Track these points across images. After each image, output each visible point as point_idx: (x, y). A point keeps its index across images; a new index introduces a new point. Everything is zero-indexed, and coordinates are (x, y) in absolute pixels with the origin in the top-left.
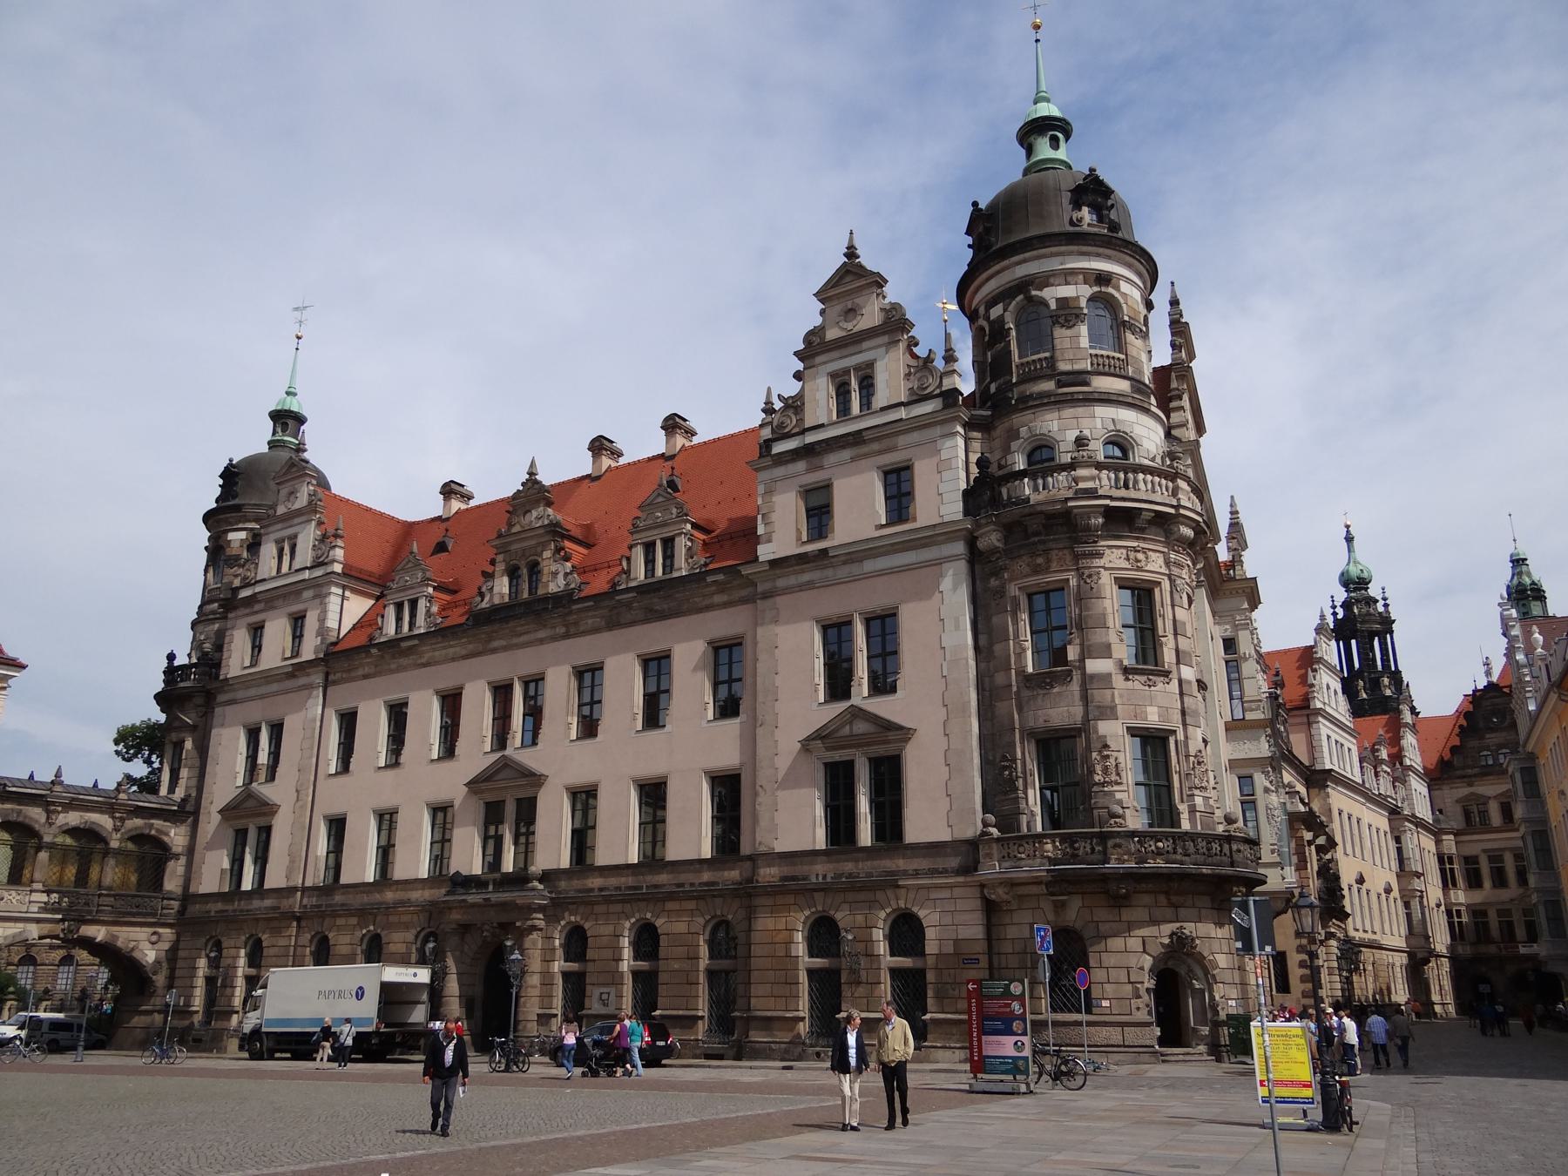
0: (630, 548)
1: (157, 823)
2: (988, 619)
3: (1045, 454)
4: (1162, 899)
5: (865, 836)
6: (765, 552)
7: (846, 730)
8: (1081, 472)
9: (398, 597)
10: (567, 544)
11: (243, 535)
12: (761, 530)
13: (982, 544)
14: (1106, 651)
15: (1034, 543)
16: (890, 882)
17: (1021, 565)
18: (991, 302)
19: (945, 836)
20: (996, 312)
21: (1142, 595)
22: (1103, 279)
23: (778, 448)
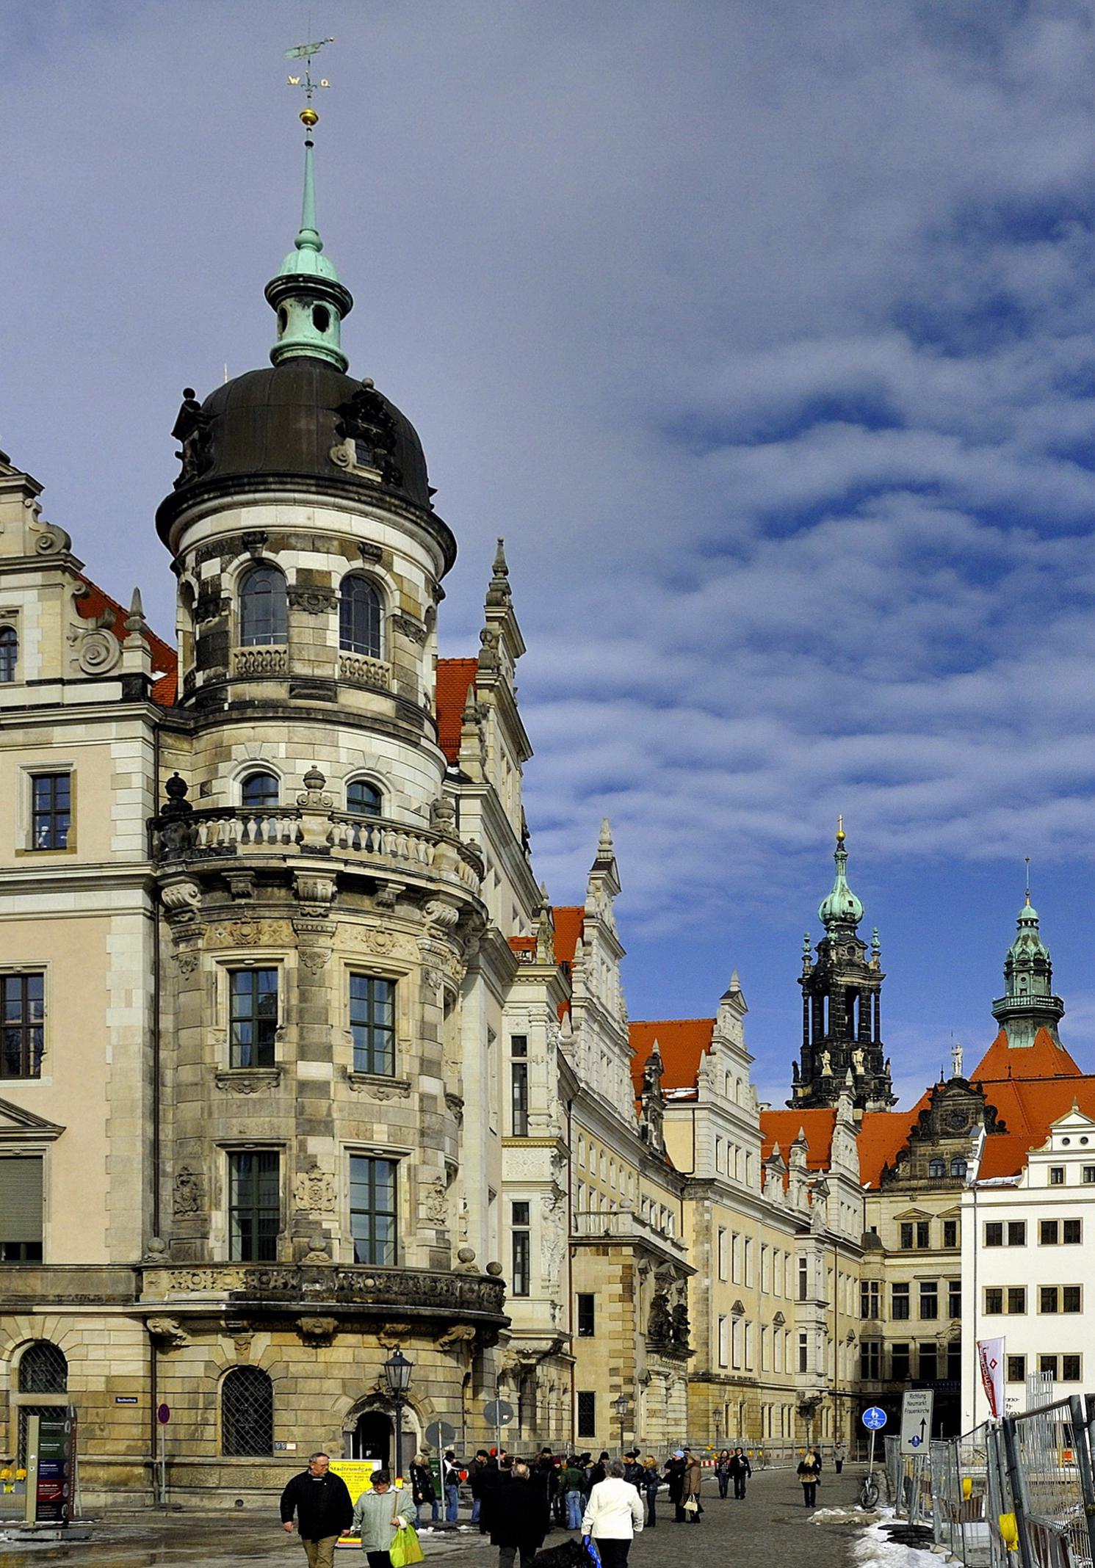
4: (372, 1339)
13: (168, 895)
15: (240, 906)
20: (211, 568)
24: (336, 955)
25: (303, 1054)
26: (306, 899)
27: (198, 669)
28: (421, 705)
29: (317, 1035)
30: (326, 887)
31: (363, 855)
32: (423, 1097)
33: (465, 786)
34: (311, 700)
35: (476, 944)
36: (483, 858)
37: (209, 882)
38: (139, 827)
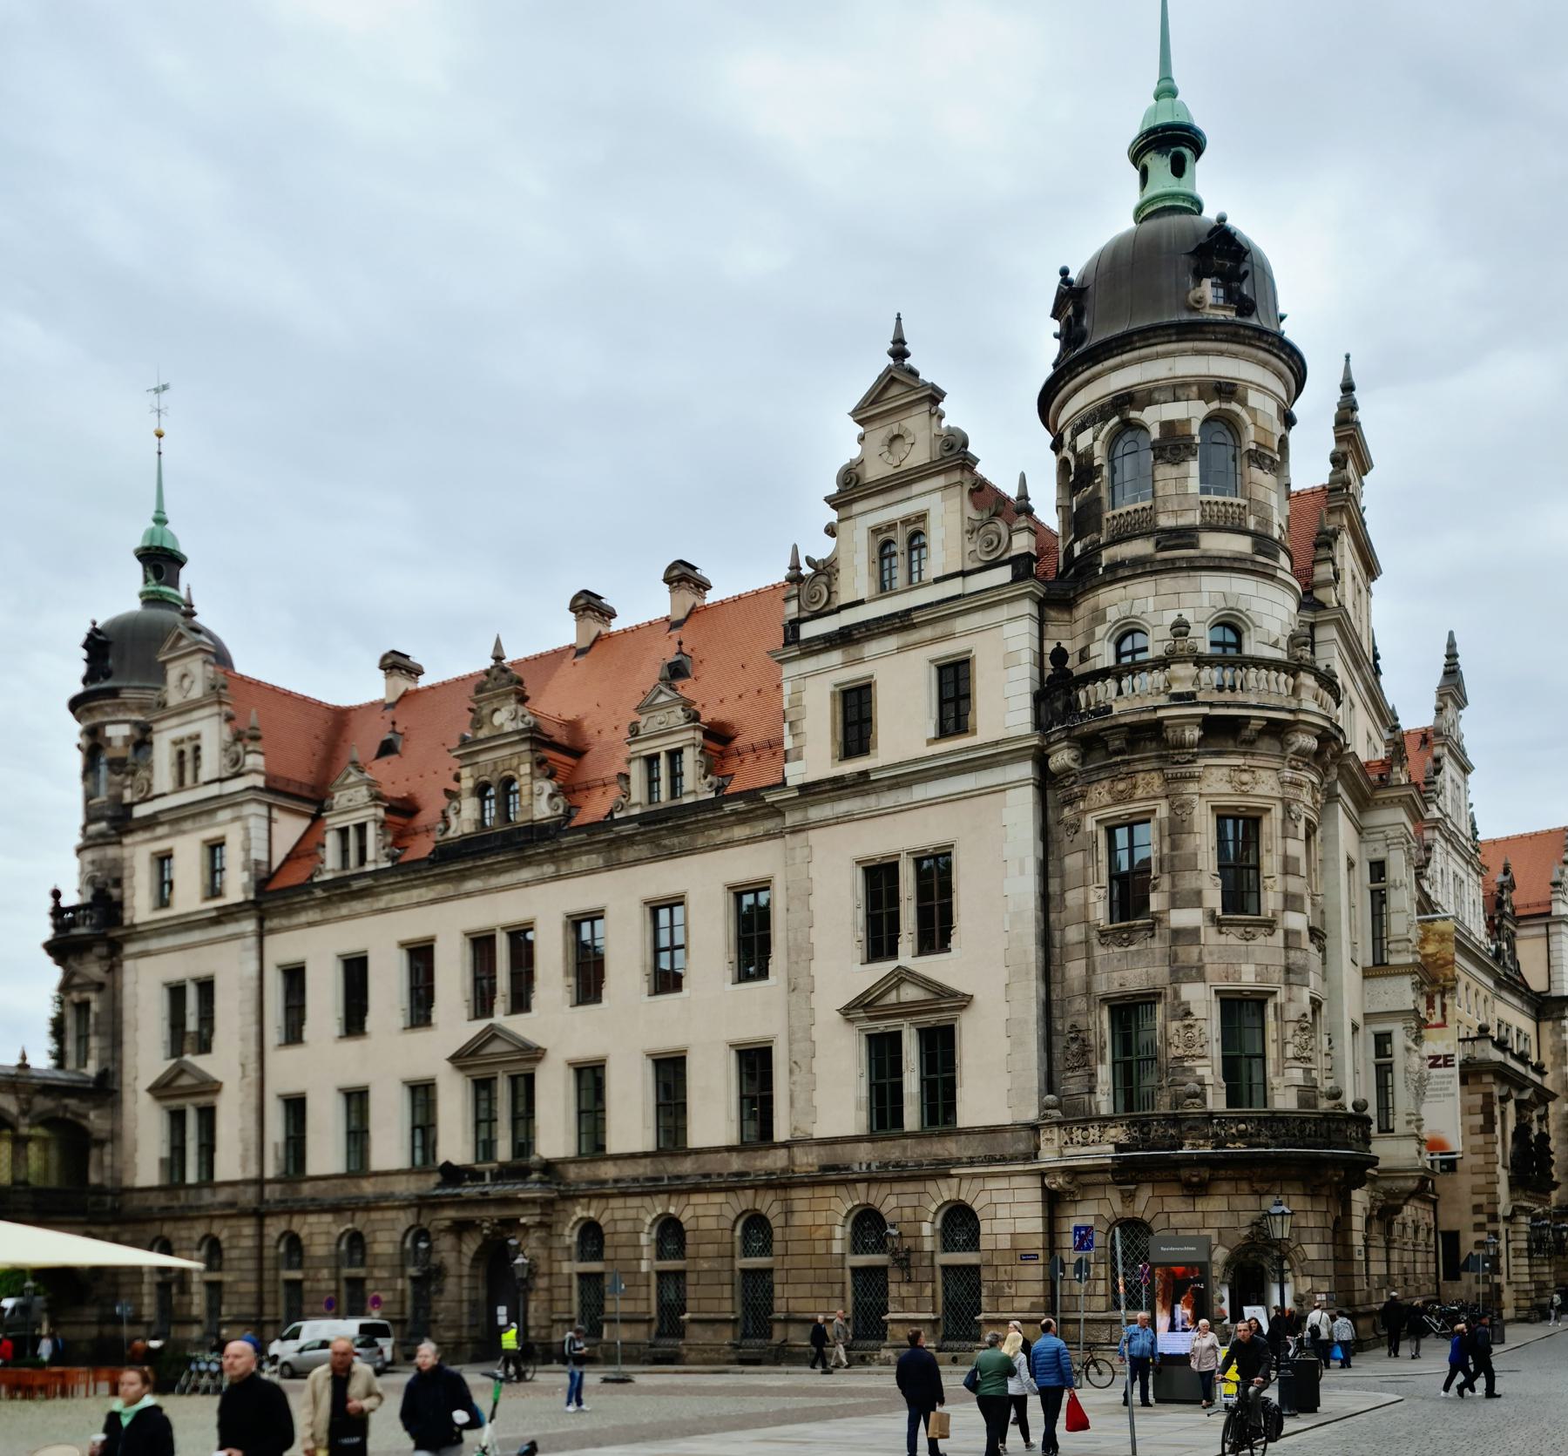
0: (629, 761)
1: (72, 1102)
2: (1061, 860)
3: (1140, 641)
5: (912, 1117)
6: (796, 774)
7: (892, 998)
8: (1178, 670)
10: (549, 754)
12: (788, 743)
14: (1196, 899)
15: (1116, 764)
16: (941, 1170)
17: (1100, 793)
18: (1079, 429)
19: (1004, 1118)
20: (1084, 440)
21: (1241, 830)
22: (1226, 390)
23: (808, 630)
24: (1204, 800)
25: (1175, 902)
26: (1174, 748)
27: (1075, 541)
28: (1276, 536)
29: (1188, 882)
30: (1192, 734)
31: (1227, 696)
32: (1287, 933)
33: (1322, 612)
34: (1176, 552)
35: (1334, 771)
36: (1339, 681)
37: (1088, 745)
38: (1027, 701)
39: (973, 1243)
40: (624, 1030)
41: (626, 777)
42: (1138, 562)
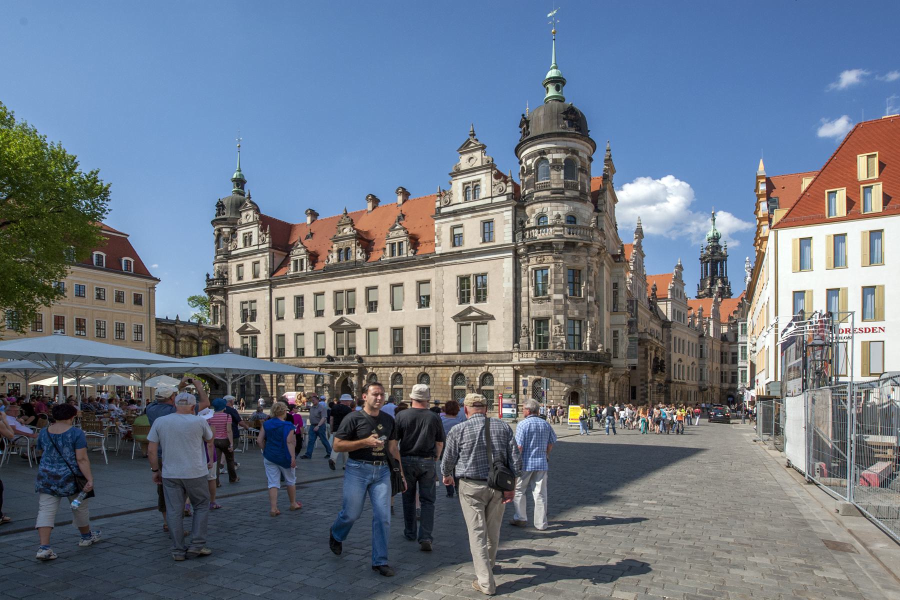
6: (438, 250)
9: (295, 258)
11: (229, 230)
12: (436, 241)
18: (529, 158)
20: (529, 162)
39: (492, 383)
40: (384, 320)
41: (385, 249)
42: (545, 197)
